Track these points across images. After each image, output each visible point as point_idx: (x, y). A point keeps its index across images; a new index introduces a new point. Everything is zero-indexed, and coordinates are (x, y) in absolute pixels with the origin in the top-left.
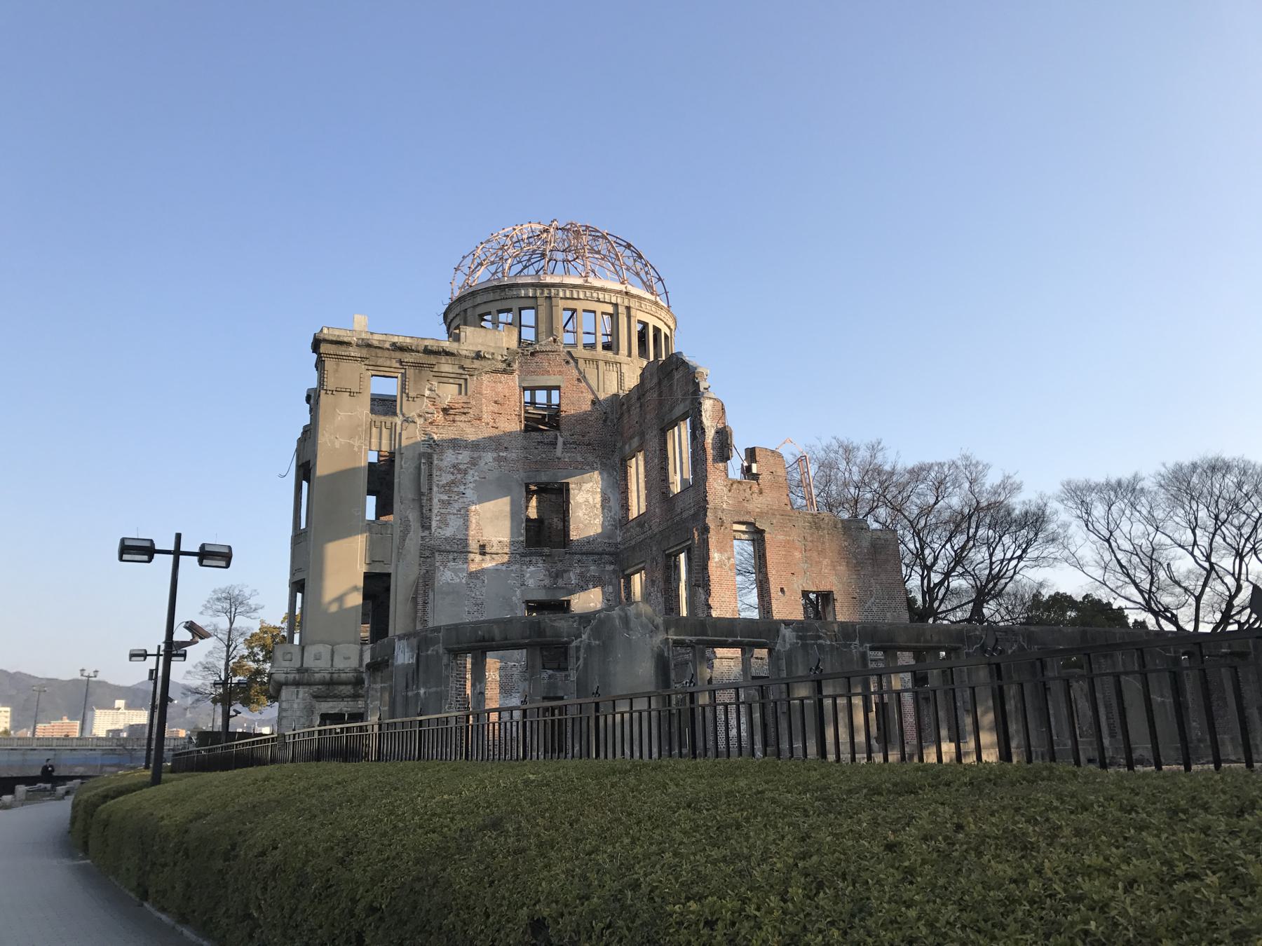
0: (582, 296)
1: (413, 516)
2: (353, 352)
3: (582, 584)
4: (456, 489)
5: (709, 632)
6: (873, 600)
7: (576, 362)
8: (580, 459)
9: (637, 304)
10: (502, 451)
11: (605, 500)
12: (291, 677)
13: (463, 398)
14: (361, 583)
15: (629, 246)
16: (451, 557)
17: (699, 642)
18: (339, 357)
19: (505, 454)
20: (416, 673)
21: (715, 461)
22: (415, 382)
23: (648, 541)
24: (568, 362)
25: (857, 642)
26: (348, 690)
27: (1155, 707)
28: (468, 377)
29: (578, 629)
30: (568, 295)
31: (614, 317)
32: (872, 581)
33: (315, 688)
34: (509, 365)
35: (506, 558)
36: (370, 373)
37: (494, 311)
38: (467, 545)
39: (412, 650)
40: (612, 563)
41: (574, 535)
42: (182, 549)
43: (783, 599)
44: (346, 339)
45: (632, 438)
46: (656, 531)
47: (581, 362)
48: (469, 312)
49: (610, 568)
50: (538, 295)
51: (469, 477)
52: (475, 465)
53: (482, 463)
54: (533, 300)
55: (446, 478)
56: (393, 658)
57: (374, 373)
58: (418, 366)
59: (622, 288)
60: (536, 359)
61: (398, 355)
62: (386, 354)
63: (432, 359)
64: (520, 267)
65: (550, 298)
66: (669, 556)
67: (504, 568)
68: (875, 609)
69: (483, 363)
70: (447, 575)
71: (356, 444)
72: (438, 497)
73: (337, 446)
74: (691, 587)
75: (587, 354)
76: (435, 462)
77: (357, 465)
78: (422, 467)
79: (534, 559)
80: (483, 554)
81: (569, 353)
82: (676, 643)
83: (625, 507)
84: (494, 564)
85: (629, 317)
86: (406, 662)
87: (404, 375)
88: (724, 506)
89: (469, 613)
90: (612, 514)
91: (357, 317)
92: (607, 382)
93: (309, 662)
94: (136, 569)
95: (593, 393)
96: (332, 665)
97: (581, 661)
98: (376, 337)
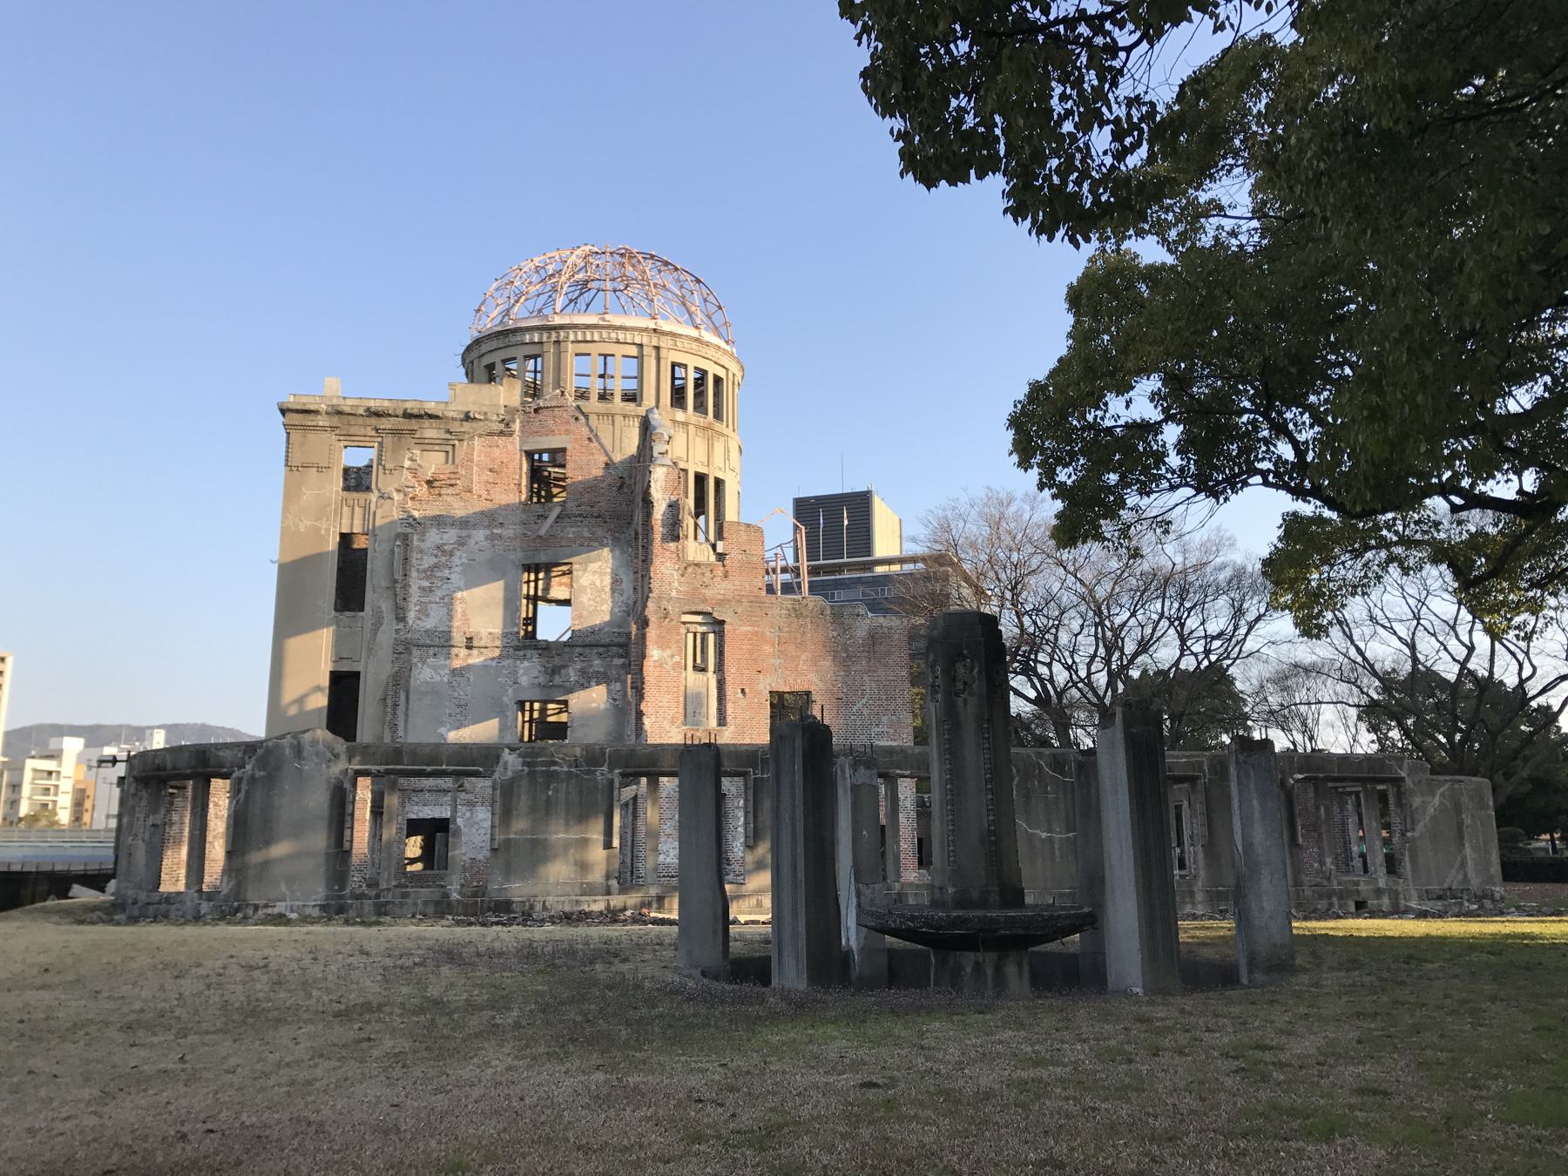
0: (596, 337)
1: (386, 606)
2: (322, 421)
4: (439, 574)
7: (586, 417)
8: (587, 534)
9: (670, 342)
10: (496, 527)
11: (616, 581)
13: (450, 468)
14: (325, 681)
16: (431, 652)
17: (388, 772)
18: (304, 428)
19: (499, 531)
21: (664, 540)
22: (393, 451)
24: (577, 419)
25: (605, 768)
28: (456, 442)
29: (243, 758)
30: (580, 338)
31: (640, 358)
32: (866, 678)
34: (507, 425)
35: (497, 653)
38: (450, 639)
40: (622, 656)
43: (743, 703)
44: (312, 407)
47: (593, 418)
49: (618, 661)
50: (545, 339)
51: (456, 560)
52: (462, 544)
53: (471, 542)
55: (428, 561)
57: (346, 443)
58: (397, 433)
59: (652, 325)
60: (540, 417)
61: (374, 421)
62: (360, 421)
63: (414, 424)
65: (558, 342)
67: (494, 664)
68: (866, 712)
69: (474, 424)
70: (425, 673)
71: (324, 526)
72: (416, 583)
73: (302, 530)
76: (416, 543)
77: (324, 550)
78: (396, 550)
79: (529, 653)
80: (469, 647)
81: (578, 407)
84: (482, 659)
85: (658, 359)
87: (381, 444)
88: (674, 594)
89: (450, 715)
90: (624, 598)
91: (327, 379)
92: (625, 440)
95: (607, 455)
97: (242, 795)
98: (349, 402)
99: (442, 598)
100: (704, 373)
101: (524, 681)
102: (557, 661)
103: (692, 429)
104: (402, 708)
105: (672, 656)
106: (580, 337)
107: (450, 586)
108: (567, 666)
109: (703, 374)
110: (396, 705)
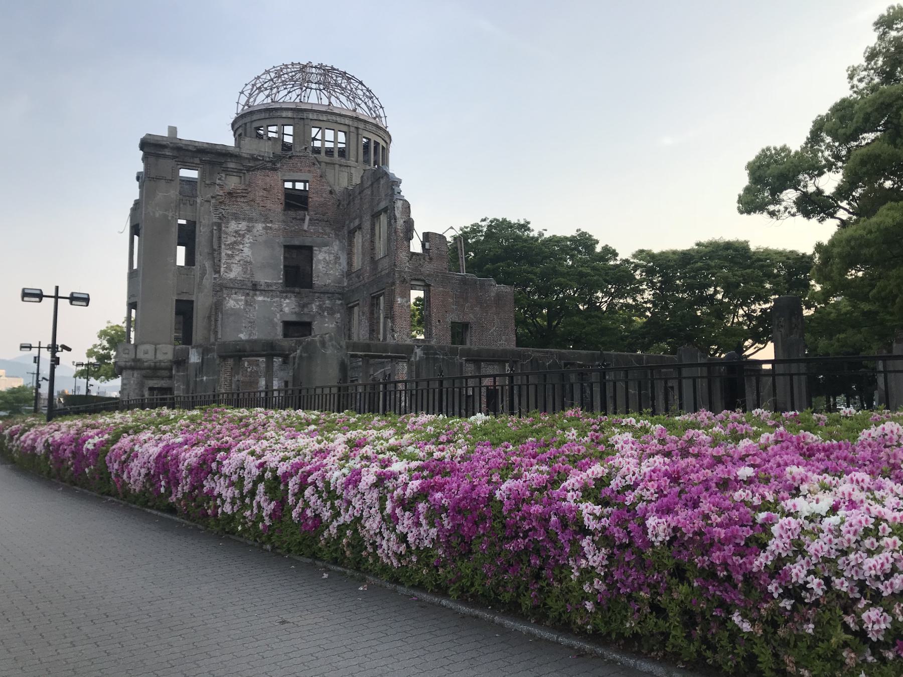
1: (207, 264)
2: (168, 152)
3: (320, 312)
4: (237, 247)
10: (268, 223)
12: (128, 364)
15: (361, 83)
16: (233, 291)
17: (366, 356)
18: (158, 156)
19: (270, 225)
20: (200, 368)
23: (362, 287)
26: (165, 373)
27: (630, 396)
32: (495, 317)
33: (144, 372)
36: (179, 167)
37: (265, 126)
39: (199, 355)
40: (340, 299)
41: (316, 281)
42: (59, 295)
45: (355, 219)
46: (367, 281)
48: (248, 125)
49: (339, 302)
51: (246, 240)
53: (255, 230)
54: (292, 120)
55: (231, 240)
56: (188, 358)
60: (292, 161)
64: (286, 92)
66: (373, 297)
68: (495, 334)
71: (170, 215)
72: (225, 252)
74: (386, 318)
75: (327, 159)
78: (215, 232)
79: (289, 295)
82: (352, 356)
83: (350, 263)
86: (196, 361)
93: (140, 355)
94: (32, 306)
96: (155, 358)
98: (184, 143)
99: (239, 261)
100: (378, 144)
102: (305, 300)
104: (219, 322)
106: (315, 118)
107: (243, 255)
108: (312, 303)
109: (377, 144)
110: (216, 320)
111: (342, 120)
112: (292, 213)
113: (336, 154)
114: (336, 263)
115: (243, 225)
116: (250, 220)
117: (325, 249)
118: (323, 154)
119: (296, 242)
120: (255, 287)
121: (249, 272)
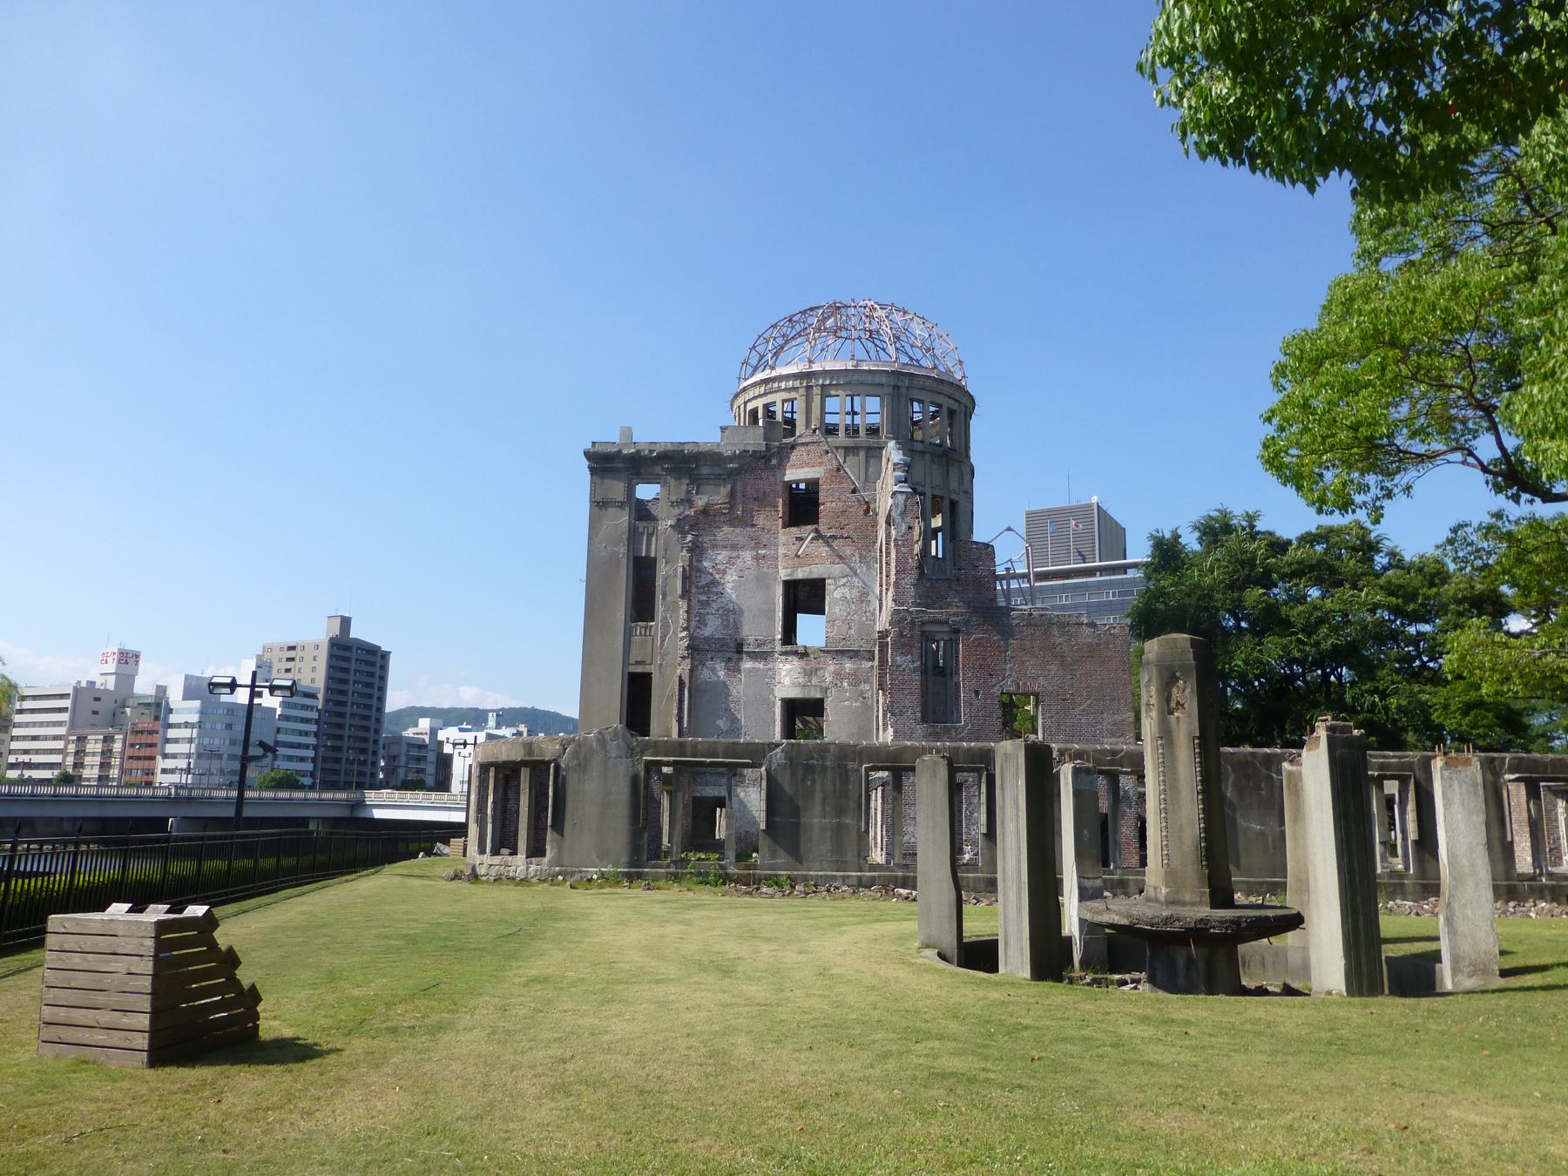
4: (715, 590)
5: (689, 753)
6: (1089, 702)
10: (761, 549)
36: (635, 481)
51: (728, 577)
76: (695, 564)
79: (790, 658)
98: (639, 448)
101: (787, 681)
103: (928, 456)
105: (913, 662)
110: (681, 701)
111: (869, 379)
112: (794, 529)
113: (862, 432)
114: (862, 602)
115: (722, 556)
116: (734, 547)
117: (844, 581)
118: (841, 433)
119: (801, 574)
120: (739, 649)
121: (731, 626)
